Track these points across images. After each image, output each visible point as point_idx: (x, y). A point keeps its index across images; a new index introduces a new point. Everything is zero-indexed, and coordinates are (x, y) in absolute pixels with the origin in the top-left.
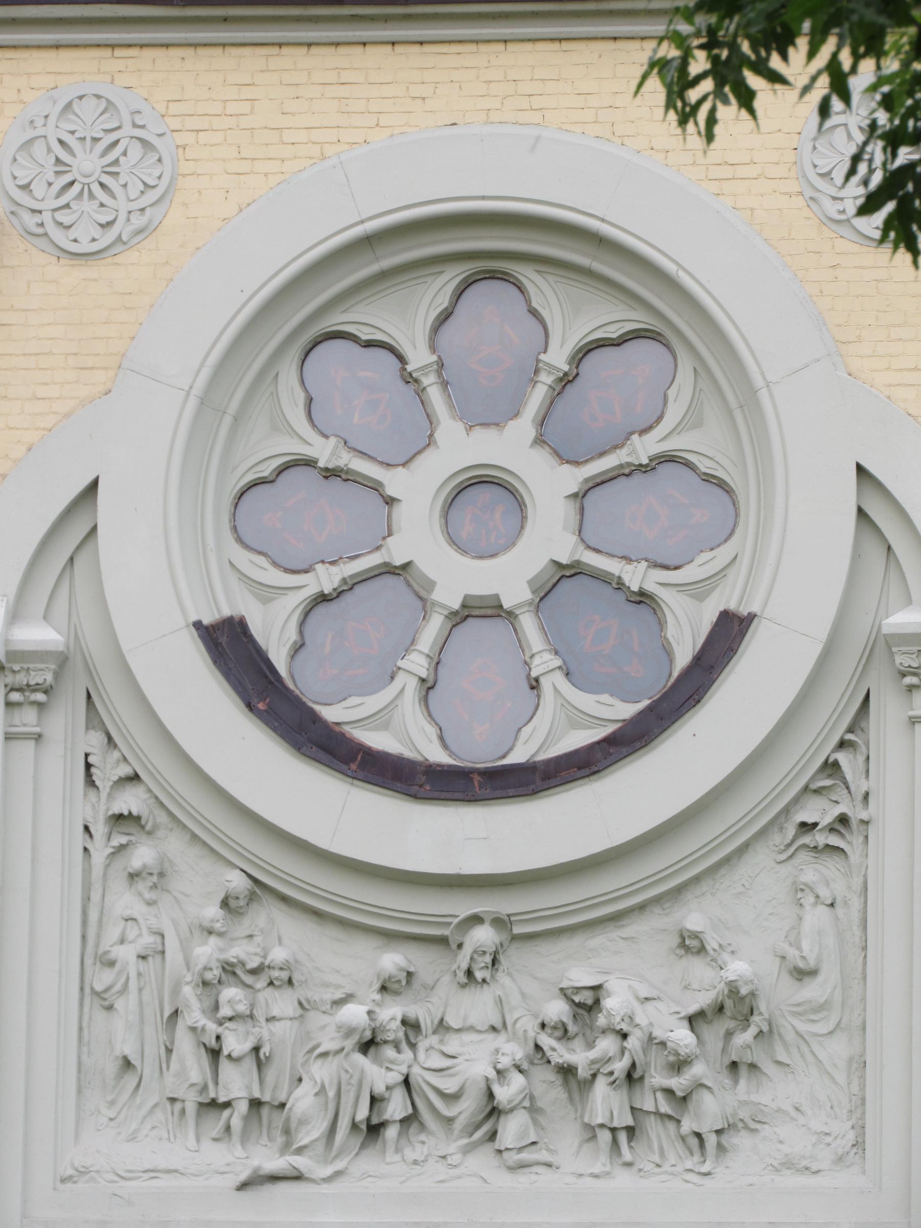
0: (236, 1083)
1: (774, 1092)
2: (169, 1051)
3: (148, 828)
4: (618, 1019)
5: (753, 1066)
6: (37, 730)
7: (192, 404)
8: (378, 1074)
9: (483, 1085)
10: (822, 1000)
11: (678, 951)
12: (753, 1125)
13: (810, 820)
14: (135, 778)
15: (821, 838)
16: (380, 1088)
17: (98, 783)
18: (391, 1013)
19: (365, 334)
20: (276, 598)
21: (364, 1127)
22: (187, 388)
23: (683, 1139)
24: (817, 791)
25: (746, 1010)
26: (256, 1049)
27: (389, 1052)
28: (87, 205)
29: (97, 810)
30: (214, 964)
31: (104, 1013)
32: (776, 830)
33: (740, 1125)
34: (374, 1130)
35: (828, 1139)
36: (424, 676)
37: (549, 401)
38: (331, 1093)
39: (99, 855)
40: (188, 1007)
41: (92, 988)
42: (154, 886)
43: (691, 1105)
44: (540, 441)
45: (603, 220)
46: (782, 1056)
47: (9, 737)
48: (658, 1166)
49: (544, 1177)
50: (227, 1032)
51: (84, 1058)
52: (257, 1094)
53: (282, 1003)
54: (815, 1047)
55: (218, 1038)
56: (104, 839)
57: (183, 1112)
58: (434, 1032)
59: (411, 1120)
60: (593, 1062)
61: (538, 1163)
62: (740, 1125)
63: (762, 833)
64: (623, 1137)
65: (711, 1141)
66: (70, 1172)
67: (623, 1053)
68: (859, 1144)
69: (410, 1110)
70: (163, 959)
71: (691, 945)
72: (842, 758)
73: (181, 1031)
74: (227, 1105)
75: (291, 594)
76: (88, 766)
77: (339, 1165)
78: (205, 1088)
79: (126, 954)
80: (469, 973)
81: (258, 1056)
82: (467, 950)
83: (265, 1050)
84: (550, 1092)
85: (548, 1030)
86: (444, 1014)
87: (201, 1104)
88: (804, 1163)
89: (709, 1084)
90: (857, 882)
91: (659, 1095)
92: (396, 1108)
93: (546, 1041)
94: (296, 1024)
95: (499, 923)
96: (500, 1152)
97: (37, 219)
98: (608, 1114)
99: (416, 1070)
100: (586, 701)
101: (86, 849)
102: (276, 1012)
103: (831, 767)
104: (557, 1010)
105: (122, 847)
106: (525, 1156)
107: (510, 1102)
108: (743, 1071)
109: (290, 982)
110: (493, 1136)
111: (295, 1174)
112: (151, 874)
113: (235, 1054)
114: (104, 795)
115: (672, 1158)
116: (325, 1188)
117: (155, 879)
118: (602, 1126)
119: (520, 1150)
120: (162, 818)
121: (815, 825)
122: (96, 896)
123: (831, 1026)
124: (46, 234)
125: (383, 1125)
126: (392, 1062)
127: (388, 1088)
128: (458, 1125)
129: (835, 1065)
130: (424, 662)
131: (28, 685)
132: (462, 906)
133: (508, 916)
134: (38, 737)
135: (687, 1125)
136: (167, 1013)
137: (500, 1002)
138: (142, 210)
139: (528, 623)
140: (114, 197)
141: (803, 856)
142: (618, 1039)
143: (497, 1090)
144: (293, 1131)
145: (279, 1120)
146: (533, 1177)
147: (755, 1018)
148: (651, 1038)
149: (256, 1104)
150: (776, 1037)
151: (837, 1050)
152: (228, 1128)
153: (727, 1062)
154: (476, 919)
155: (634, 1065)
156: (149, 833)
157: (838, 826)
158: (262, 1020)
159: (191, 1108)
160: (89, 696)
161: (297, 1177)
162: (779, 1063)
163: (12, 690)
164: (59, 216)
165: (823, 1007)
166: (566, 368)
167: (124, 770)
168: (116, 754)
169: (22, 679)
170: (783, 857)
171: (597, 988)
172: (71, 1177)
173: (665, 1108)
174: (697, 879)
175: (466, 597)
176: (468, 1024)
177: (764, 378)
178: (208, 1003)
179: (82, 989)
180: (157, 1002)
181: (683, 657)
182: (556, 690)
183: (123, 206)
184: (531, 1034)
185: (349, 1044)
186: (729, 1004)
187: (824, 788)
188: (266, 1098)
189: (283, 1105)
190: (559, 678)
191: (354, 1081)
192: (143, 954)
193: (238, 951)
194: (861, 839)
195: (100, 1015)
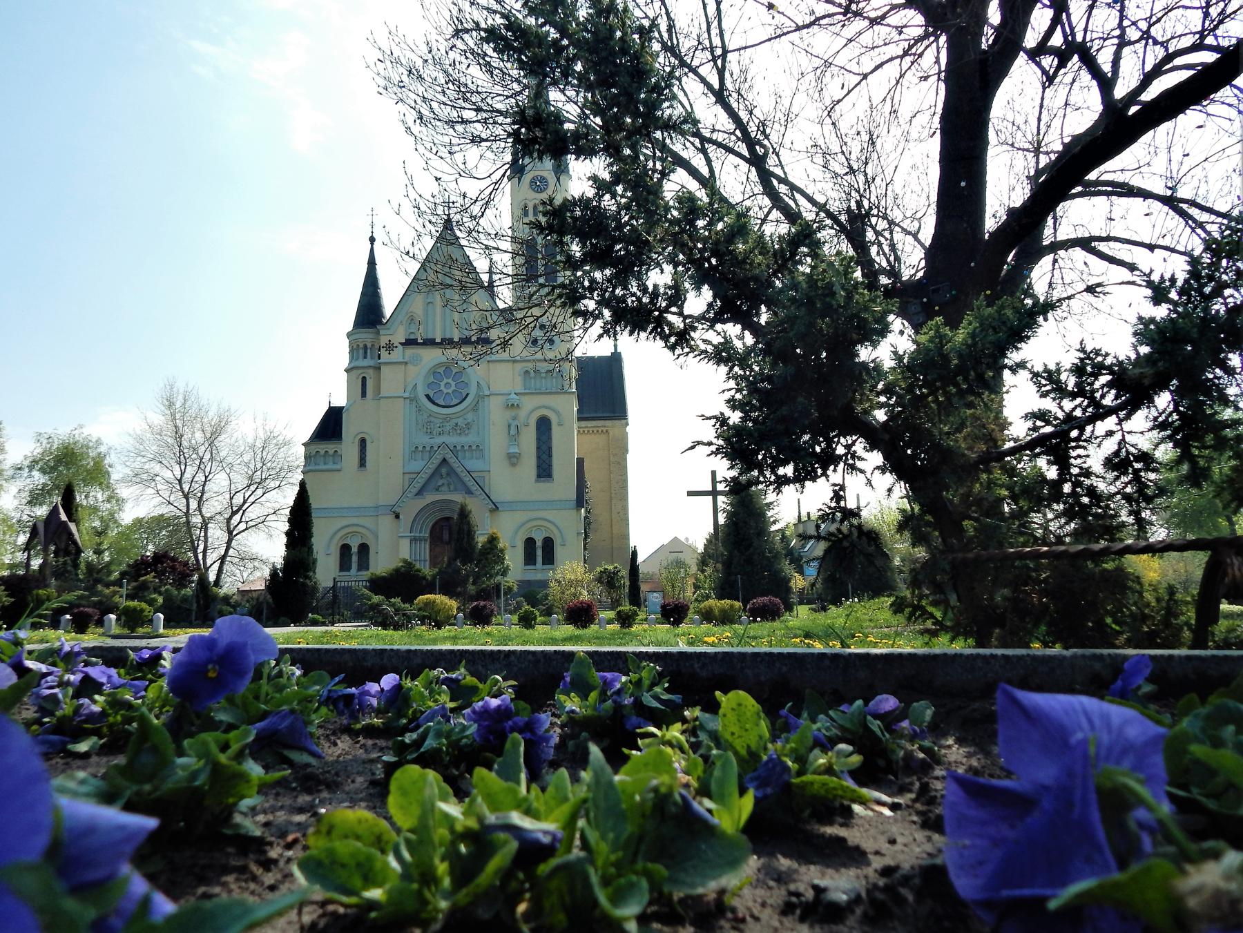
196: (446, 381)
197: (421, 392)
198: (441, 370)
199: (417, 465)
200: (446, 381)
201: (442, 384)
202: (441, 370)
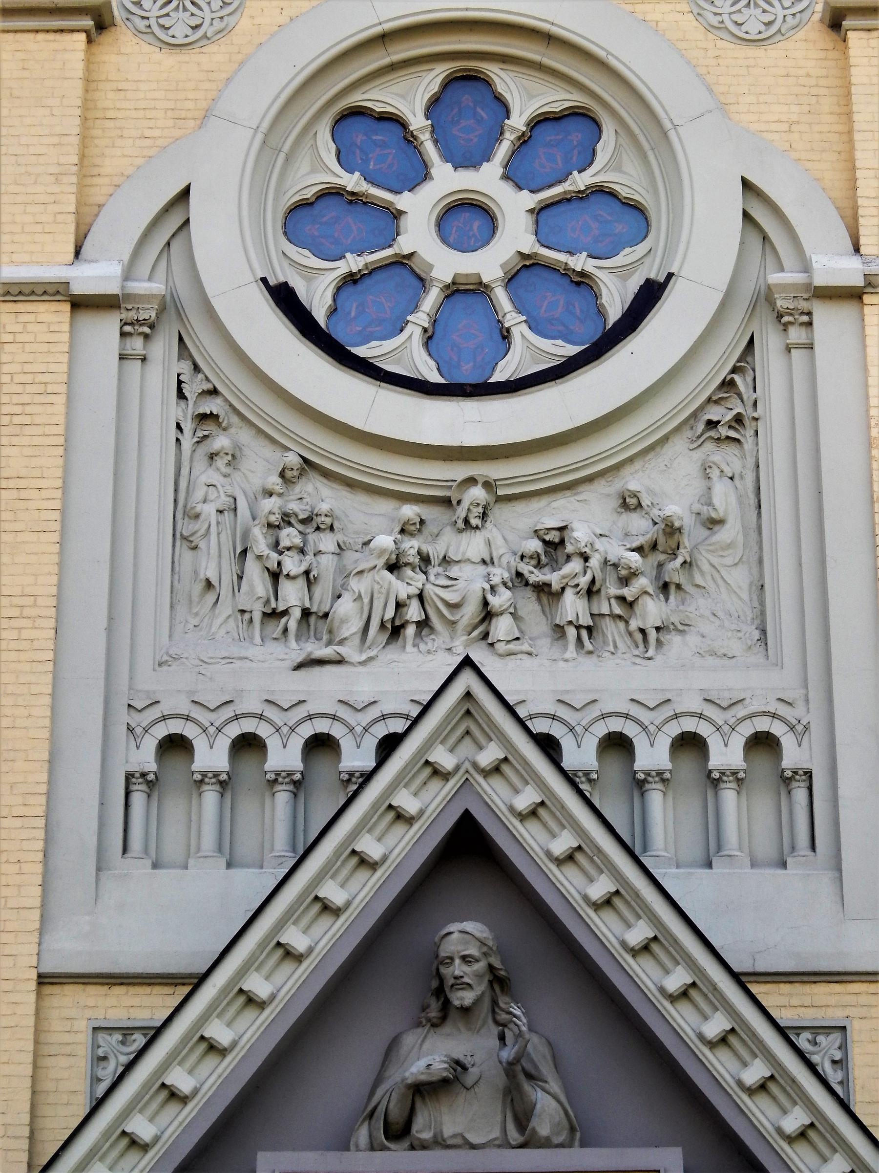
0: (292, 595)
2: (240, 578)
3: (224, 425)
4: (583, 544)
5: (678, 586)
6: (144, 352)
7: (260, 137)
8: (402, 587)
9: (480, 594)
10: (729, 541)
11: (619, 510)
12: (681, 627)
13: (715, 419)
14: (214, 392)
15: (724, 431)
16: (403, 596)
17: (187, 394)
18: (411, 546)
19: (379, 108)
20: (315, 278)
21: (389, 626)
22: (255, 127)
23: (630, 634)
24: (717, 402)
25: (674, 546)
26: (307, 573)
27: (408, 572)
28: (181, 14)
29: (185, 414)
30: (276, 510)
31: (191, 553)
32: (688, 427)
33: (672, 627)
34: (395, 631)
35: (740, 635)
36: (426, 325)
37: (510, 153)
38: (366, 600)
39: (187, 442)
40: (257, 541)
41: (181, 535)
42: (229, 464)
43: (638, 609)
44: (506, 177)
45: (553, 24)
46: (699, 580)
47: (122, 357)
48: (613, 653)
49: (527, 661)
50: (286, 558)
51: (176, 582)
52: (307, 605)
53: (327, 542)
54: (724, 573)
55: (279, 564)
56: (191, 433)
57: (251, 620)
58: (439, 565)
59: (424, 624)
60: (564, 577)
61: (522, 652)
62: (672, 627)
63: (677, 429)
64: (584, 634)
65: (652, 635)
66: (165, 658)
67: (585, 573)
69: (424, 617)
70: (236, 515)
71: (629, 503)
72: (737, 378)
73: (251, 563)
74: (285, 613)
75: (327, 273)
76: (180, 383)
77: (372, 653)
78: (268, 602)
79: (209, 510)
80: (466, 521)
82: (465, 504)
83: (314, 573)
84: (529, 605)
85: (525, 560)
86: (447, 551)
87: (265, 614)
88: (723, 651)
89: (652, 592)
90: (750, 462)
91: (613, 601)
92: (414, 612)
93: (525, 568)
94: (336, 558)
95: (488, 485)
96: (492, 645)
97: (146, 22)
98: (575, 616)
99: (429, 587)
100: (545, 344)
101: (178, 440)
102: (322, 548)
103: (728, 385)
104: (535, 545)
105: (205, 437)
106: (512, 647)
107: (501, 606)
108: (672, 589)
109: (331, 528)
110: (485, 636)
111: (338, 658)
112: (227, 454)
113: (292, 574)
114: (191, 403)
116: (360, 669)
117: (230, 458)
119: (508, 642)
120: (235, 419)
121: (718, 422)
122: (185, 471)
123: (737, 561)
124: (153, 33)
125: (403, 626)
126: (411, 579)
127: (409, 597)
128: (461, 626)
129: (740, 587)
130: (425, 317)
131: (137, 320)
132: (459, 471)
133: (495, 481)
134: (144, 359)
135: (634, 624)
136: (239, 550)
137: (489, 543)
138: (222, 18)
139: (501, 296)
140: (201, 10)
141: (709, 446)
142: (582, 561)
143: (490, 598)
144: (335, 630)
145: (323, 626)
146: (518, 661)
147: (682, 550)
148: (606, 561)
149: (306, 613)
150: (695, 568)
151: (740, 578)
152: (285, 630)
153: (661, 583)
154: (471, 481)
155: (593, 581)
156: (225, 429)
157: (734, 424)
158: (312, 554)
159: (257, 617)
160: (181, 339)
161: (340, 661)
162: (698, 586)
163: (126, 324)
164: (162, 21)
165: (730, 546)
166: (524, 129)
167: (207, 386)
168: (200, 376)
169: (132, 315)
170: (695, 445)
171: (562, 529)
172: (167, 661)
173: (618, 610)
174: (631, 460)
175: (456, 275)
176: (466, 557)
177: (672, 123)
178: (271, 540)
179: (174, 535)
180: (231, 543)
181: (614, 313)
182: (523, 335)
183: (208, 16)
185: (381, 562)
186: (662, 540)
187: (722, 398)
188: (314, 609)
189: (326, 615)
190: (524, 328)
192: (221, 509)
193: (293, 506)
194: (752, 432)
195: (187, 556)
196: (446, 180)
197: (232, 259)
198: (410, 98)
199: (175, 904)
200: (446, 180)
201: (419, 208)
202: (410, 98)
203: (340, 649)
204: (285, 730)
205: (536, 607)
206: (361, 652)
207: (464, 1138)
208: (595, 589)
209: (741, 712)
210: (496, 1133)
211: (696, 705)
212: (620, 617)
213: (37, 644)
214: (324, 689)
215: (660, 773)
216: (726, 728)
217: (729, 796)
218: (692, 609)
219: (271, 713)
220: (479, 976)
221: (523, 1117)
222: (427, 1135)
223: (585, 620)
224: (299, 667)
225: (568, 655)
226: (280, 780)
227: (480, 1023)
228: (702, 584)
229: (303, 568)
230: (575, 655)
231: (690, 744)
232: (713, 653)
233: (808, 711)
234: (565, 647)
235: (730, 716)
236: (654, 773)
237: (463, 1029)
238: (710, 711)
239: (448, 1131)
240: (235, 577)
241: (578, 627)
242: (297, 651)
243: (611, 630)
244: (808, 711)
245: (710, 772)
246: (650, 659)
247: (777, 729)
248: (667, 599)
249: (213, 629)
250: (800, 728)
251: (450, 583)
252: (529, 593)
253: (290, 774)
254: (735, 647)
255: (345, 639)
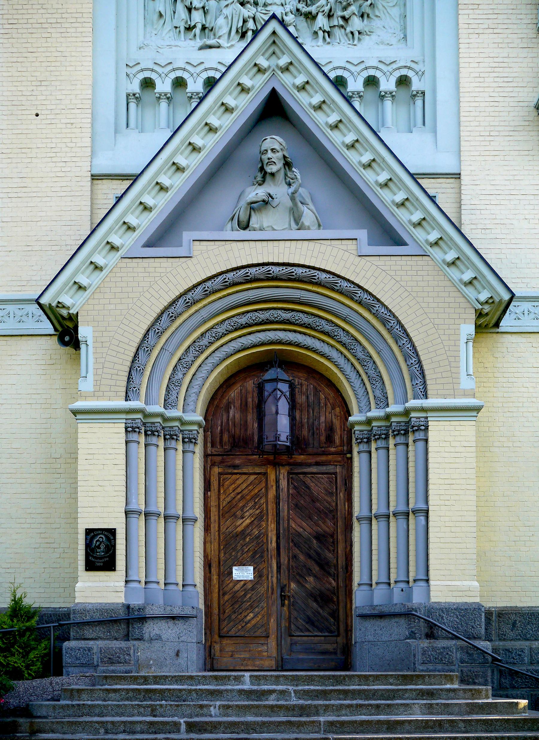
1: (376, 23)
2: (174, 12)
5: (368, 16)
12: (369, 33)
21: (240, 31)
23: (347, 35)
26: (203, 8)
35: (395, 35)
46: (377, 13)
48: (339, 43)
51: (146, 14)
52: (204, 23)
55: (191, 3)
64: (326, 34)
65: (356, 34)
66: (142, 45)
68: (405, 38)
74: (195, 26)
78: (186, 22)
81: (205, 11)
84: (302, 22)
87: (185, 27)
92: (251, 25)
99: (258, 14)
108: (365, 16)
111: (218, 45)
115: (343, 41)
116: (227, 50)
118: (320, 28)
135: (348, 29)
149: (204, 28)
159: (182, 29)
161: (219, 47)
162: (377, 16)
184: (295, 4)
189: (213, 28)
191: (238, 13)
203: (218, 40)
204: (195, 75)
205: (305, 24)
206: (228, 43)
207: (272, 227)
208: (331, 14)
209: (394, 66)
210: (287, 226)
211: (375, 63)
212: (342, 27)
213: (84, 34)
214: (212, 58)
215: (358, 93)
216: (388, 73)
217: (388, 103)
218: (374, 24)
219: (188, 67)
220: (279, 159)
221: (297, 218)
222: (256, 226)
223: (327, 29)
224: (201, 48)
225: (319, 44)
226: (193, 97)
227: (279, 182)
228: (379, 15)
229: (201, 5)
230: (322, 44)
231: (371, 82)
232: (382, 43)
233: (424, 66)
234: (318, 42)
235: (390, 68)
236: (356, 93)
237: (272, 185)
238: (381, 66)
239: (265, 225)
240: (172, 12)
241: (324, 31)
242: (199, 42)
243: (338, 32)
244: (424, 66)
245: (381, 92)
246: (355, 45)
247: (410, 74)
248: (363, 21)
249: (163, 35)
250: (420, 73)
251: (267, 12)
252: (302, 18)
253: (198, 94)
254: (394, 41)
255: (221, 36)
